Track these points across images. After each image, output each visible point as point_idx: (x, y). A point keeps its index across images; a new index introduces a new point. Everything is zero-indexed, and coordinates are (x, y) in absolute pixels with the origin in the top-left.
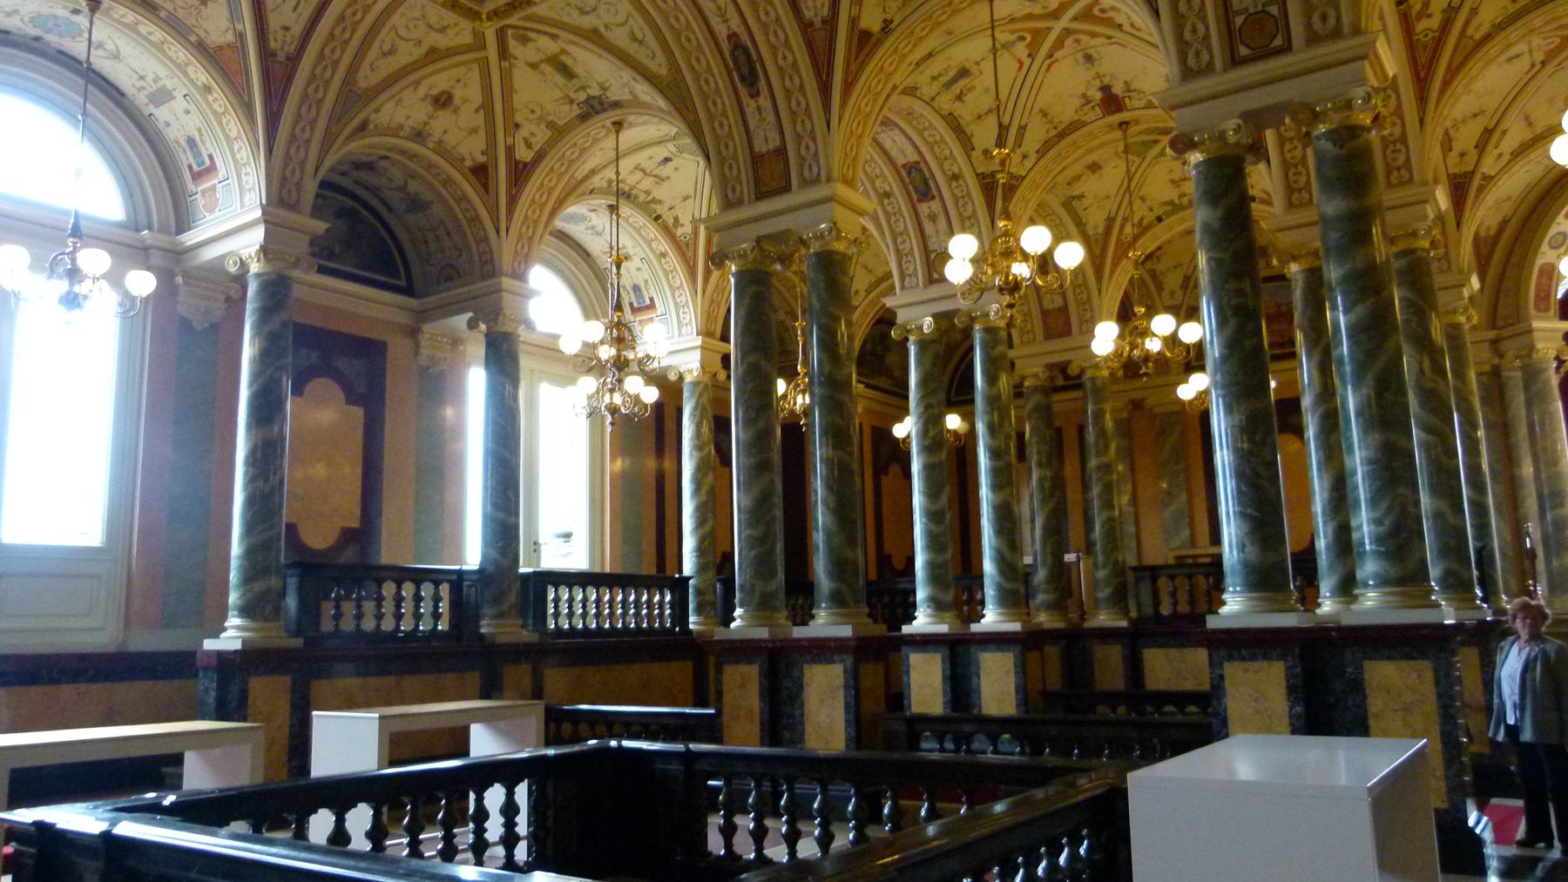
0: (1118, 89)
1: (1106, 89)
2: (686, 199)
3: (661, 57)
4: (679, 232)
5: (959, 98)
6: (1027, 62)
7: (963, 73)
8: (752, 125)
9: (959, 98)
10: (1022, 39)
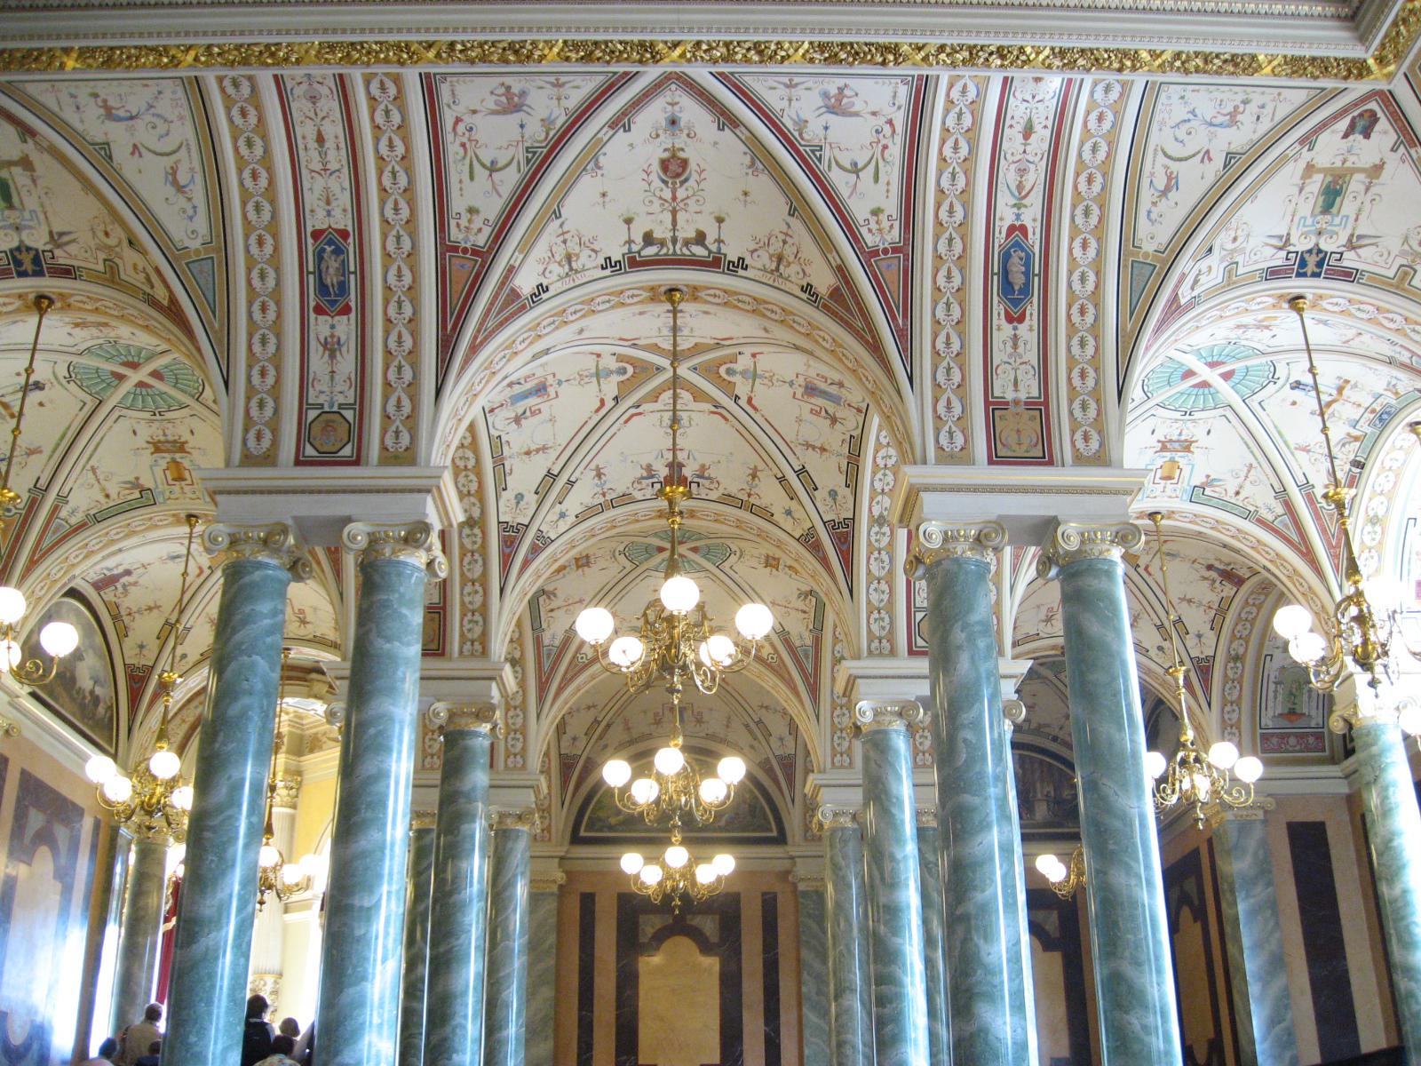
0: (687, 472)
1: (675, 466)
3: (201, 224)
5: (517, 420)
6: (610, 403)
7: (541, 389)
9: (517, 420)
10: (624, 371)
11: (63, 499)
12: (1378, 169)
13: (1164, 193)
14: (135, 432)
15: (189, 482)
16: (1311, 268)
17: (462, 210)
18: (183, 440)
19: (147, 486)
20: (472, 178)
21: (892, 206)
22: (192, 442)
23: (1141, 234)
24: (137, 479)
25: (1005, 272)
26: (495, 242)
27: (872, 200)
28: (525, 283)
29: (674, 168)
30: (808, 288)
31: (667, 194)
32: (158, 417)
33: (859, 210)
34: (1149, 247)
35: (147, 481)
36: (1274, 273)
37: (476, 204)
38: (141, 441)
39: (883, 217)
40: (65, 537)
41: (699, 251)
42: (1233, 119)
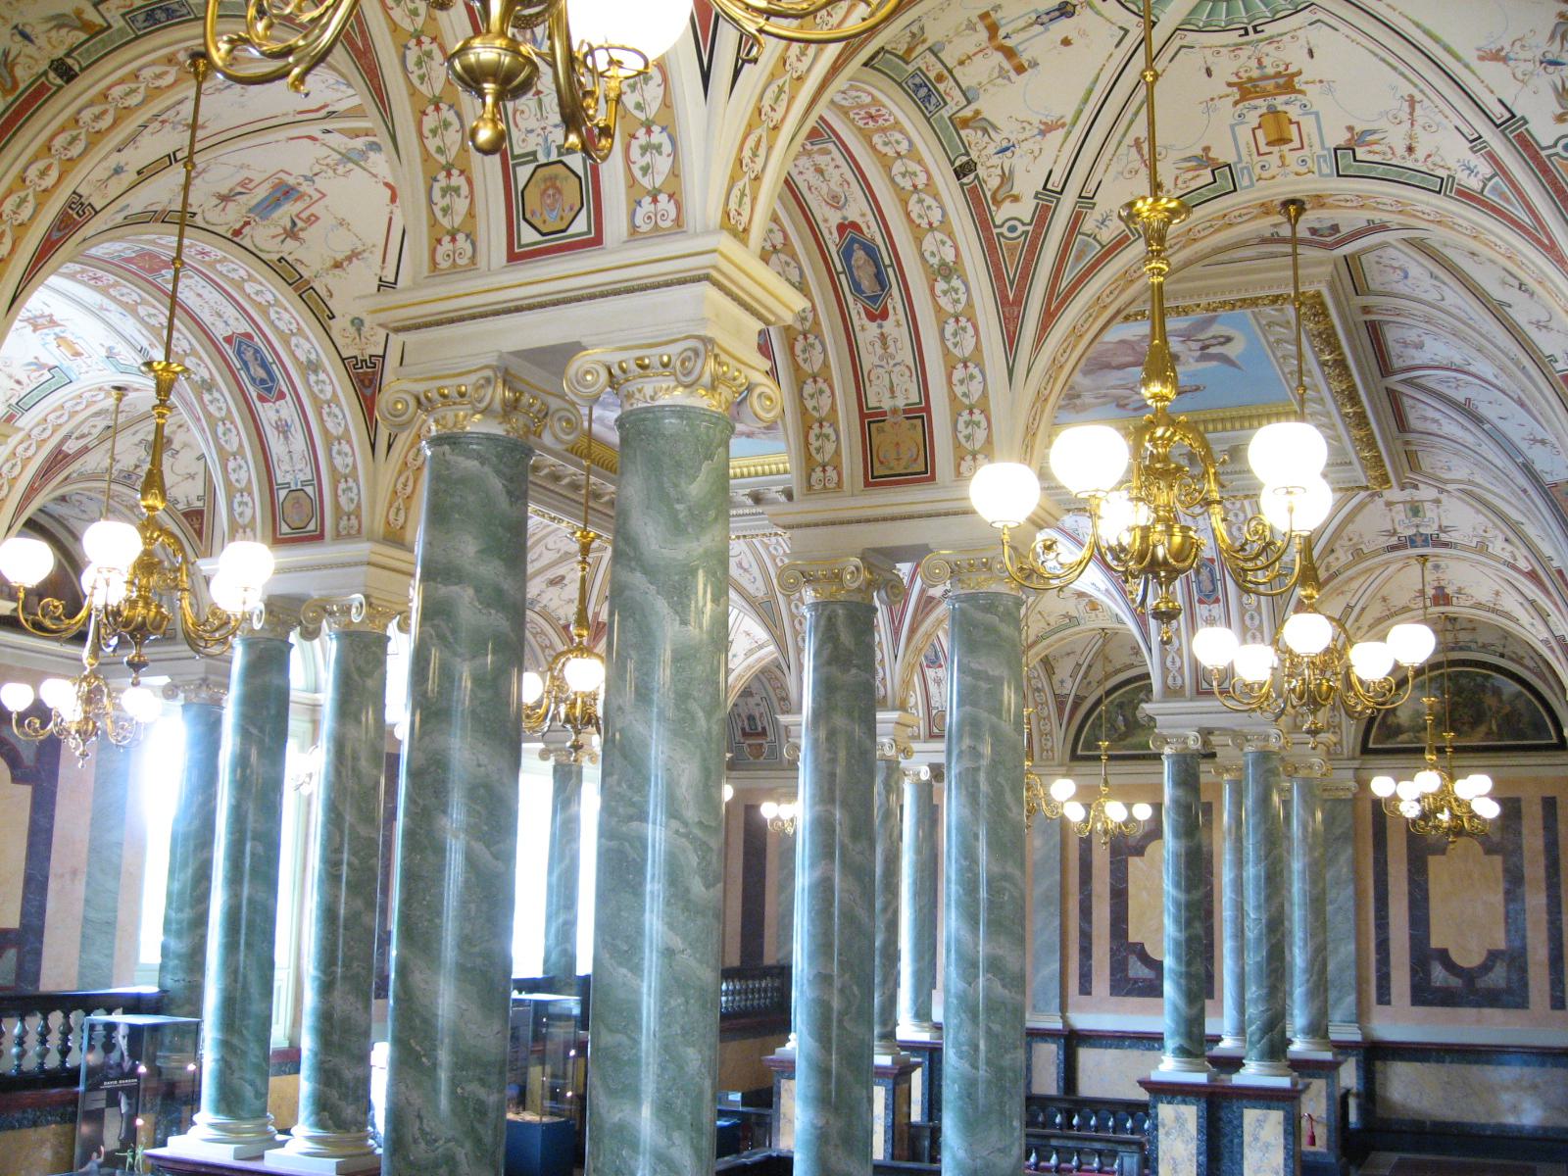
2: (1046, 129)
4: (1003, 213)
11: (1086, 201)
14: (1209, 72)
15: (1296, 144)
18: (1292, 69)
19: (1222, 160)
22: (1310, 70)
24: (1207, 149)
32: (1252, 36)
35: (1223, 153)
38: (1218, 85)
40: (1094, 266)
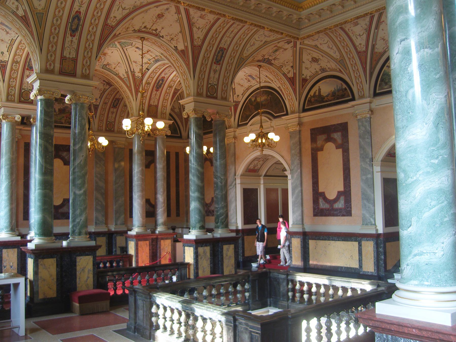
8: (66, 45)
12: (286, 49)
13: (251, 46)
16: (265, 61)
17: (112, 17)
20: (118, 10)
21: (202, 38)
23: (244, 53)
25: (217, 56)
26: (117, 25)
27: (198, 35)
28: (118, 33)
29: (160, 16)
30: (176, 47)
31: (155, 20)
33: (196, 36)
34: (245, 55)
36: (259, 61)
37: (115, 16)
39: (199, 39)
41: (154, 32)
42: (269, 36)
